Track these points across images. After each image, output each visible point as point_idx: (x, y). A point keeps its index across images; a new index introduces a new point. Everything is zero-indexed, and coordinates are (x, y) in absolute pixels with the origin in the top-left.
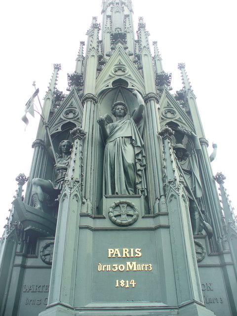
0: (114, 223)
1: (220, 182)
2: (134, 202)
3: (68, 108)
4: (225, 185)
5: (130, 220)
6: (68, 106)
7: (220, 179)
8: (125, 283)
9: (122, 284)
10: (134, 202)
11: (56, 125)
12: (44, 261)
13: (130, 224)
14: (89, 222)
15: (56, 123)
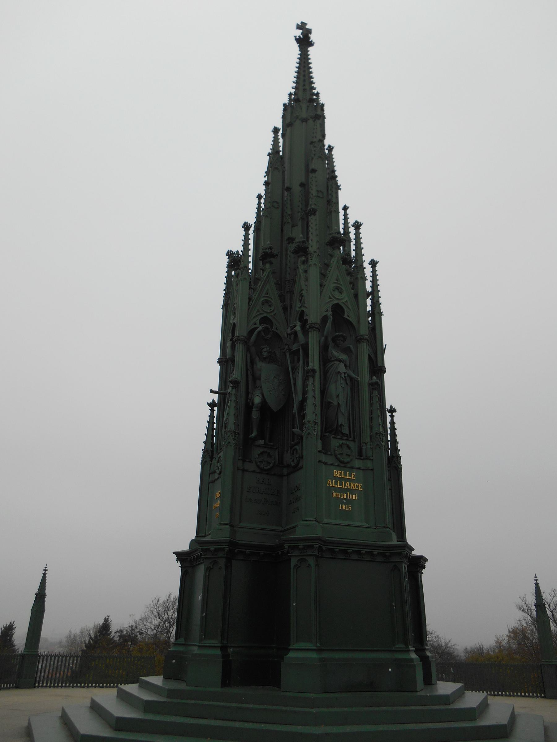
0: (339, 460)
1: (392, 416)
2: (352, 445)
3: (264, 297)
4: (395, 419)
5: (349, 459)
6: (263, 295)
7: (392, 411)
8: (346, 507)
9: (344, 508)
10: (352, 445)
11: (254, 317)
12: (258, 466)
13: (348, 463)
14: (323, 458)
15: (254, 315)
